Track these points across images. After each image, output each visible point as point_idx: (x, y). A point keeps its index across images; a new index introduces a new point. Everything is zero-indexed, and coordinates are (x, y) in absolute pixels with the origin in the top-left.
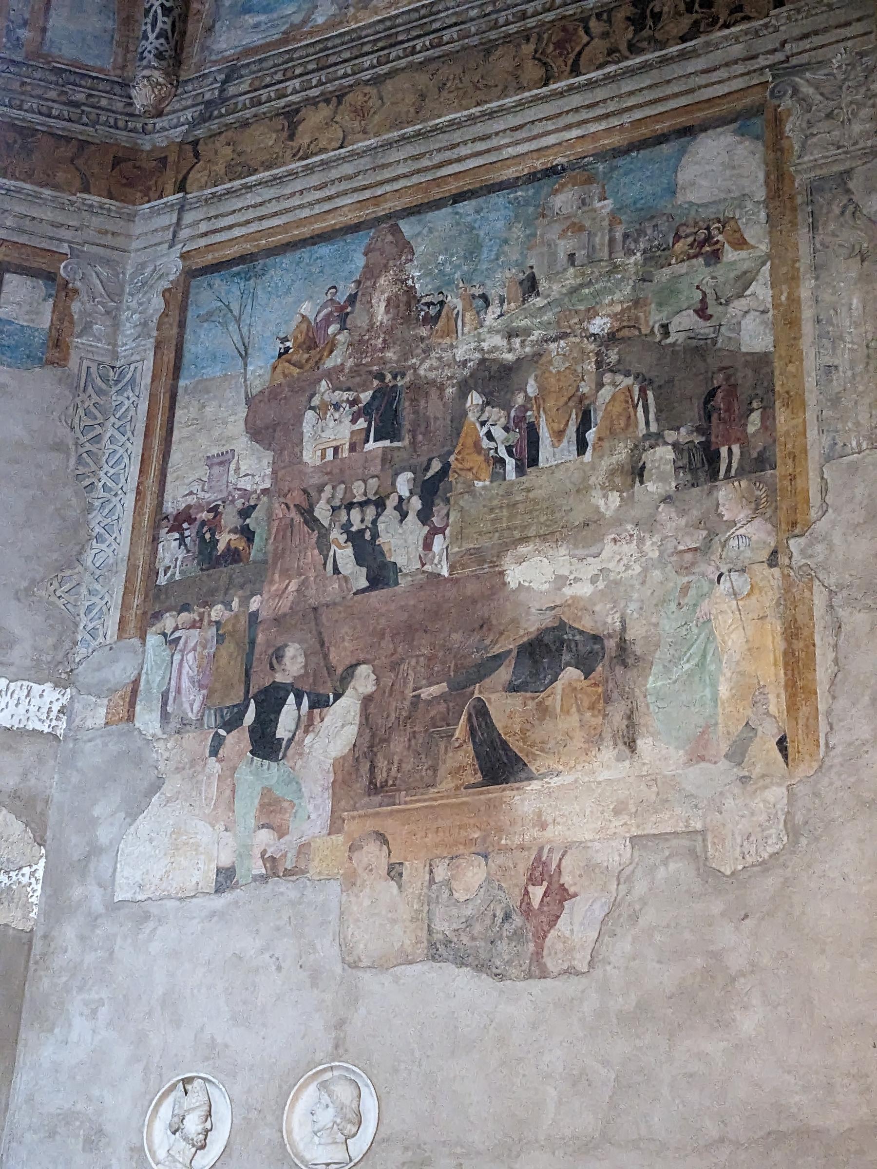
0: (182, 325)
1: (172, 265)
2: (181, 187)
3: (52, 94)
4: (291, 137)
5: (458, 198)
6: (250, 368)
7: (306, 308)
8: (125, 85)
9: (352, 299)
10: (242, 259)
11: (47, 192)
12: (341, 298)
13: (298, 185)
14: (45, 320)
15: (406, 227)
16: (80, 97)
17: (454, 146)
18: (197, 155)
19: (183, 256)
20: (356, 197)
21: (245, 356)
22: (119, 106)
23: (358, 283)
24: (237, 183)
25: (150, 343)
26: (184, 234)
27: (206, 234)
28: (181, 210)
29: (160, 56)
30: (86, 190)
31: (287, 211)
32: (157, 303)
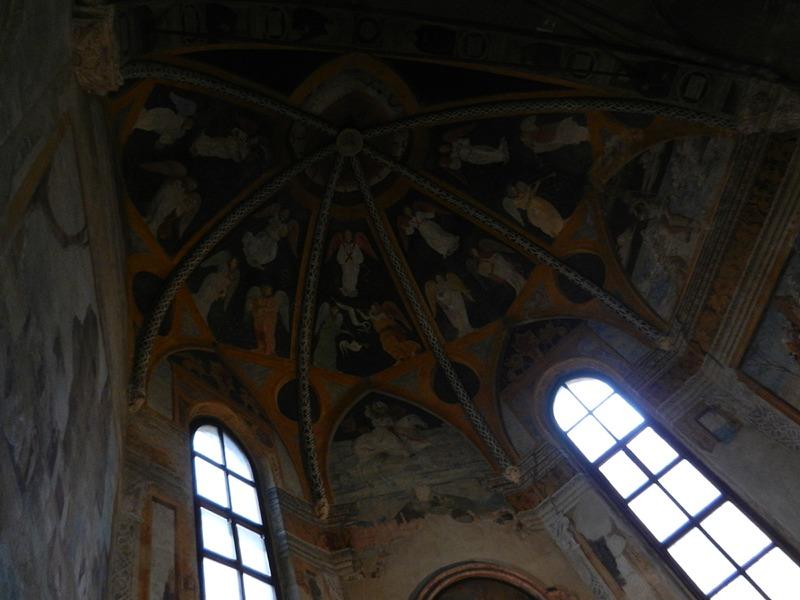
0: (756, 382)
1: (730, 372)
2: (704, 353)
4: (714, 311)
5: (783, 272)
6: (792, 370)
7: (784, 341)
8: (658, 349)
9: (793, 325)
10: (747, 350)
11: (679, 391)
12: (791, 328)
13: (734, 318)
14: (723, 420)
15: (780, 293)
16: (653, 363)
17: (761, 265)
18: (697, 343)
19: (730, 366)
20: (754, 303)
21: (786, 370)
22: (663, 355)
23: (789, 319)
24: (717, 336)
25: (755, 396)
26: (722, 362)
27: (728, 356)
28: (712, 357)
29: (657, 334)
30: (685, 380)
31: (741, 326)
32: (741, 384)
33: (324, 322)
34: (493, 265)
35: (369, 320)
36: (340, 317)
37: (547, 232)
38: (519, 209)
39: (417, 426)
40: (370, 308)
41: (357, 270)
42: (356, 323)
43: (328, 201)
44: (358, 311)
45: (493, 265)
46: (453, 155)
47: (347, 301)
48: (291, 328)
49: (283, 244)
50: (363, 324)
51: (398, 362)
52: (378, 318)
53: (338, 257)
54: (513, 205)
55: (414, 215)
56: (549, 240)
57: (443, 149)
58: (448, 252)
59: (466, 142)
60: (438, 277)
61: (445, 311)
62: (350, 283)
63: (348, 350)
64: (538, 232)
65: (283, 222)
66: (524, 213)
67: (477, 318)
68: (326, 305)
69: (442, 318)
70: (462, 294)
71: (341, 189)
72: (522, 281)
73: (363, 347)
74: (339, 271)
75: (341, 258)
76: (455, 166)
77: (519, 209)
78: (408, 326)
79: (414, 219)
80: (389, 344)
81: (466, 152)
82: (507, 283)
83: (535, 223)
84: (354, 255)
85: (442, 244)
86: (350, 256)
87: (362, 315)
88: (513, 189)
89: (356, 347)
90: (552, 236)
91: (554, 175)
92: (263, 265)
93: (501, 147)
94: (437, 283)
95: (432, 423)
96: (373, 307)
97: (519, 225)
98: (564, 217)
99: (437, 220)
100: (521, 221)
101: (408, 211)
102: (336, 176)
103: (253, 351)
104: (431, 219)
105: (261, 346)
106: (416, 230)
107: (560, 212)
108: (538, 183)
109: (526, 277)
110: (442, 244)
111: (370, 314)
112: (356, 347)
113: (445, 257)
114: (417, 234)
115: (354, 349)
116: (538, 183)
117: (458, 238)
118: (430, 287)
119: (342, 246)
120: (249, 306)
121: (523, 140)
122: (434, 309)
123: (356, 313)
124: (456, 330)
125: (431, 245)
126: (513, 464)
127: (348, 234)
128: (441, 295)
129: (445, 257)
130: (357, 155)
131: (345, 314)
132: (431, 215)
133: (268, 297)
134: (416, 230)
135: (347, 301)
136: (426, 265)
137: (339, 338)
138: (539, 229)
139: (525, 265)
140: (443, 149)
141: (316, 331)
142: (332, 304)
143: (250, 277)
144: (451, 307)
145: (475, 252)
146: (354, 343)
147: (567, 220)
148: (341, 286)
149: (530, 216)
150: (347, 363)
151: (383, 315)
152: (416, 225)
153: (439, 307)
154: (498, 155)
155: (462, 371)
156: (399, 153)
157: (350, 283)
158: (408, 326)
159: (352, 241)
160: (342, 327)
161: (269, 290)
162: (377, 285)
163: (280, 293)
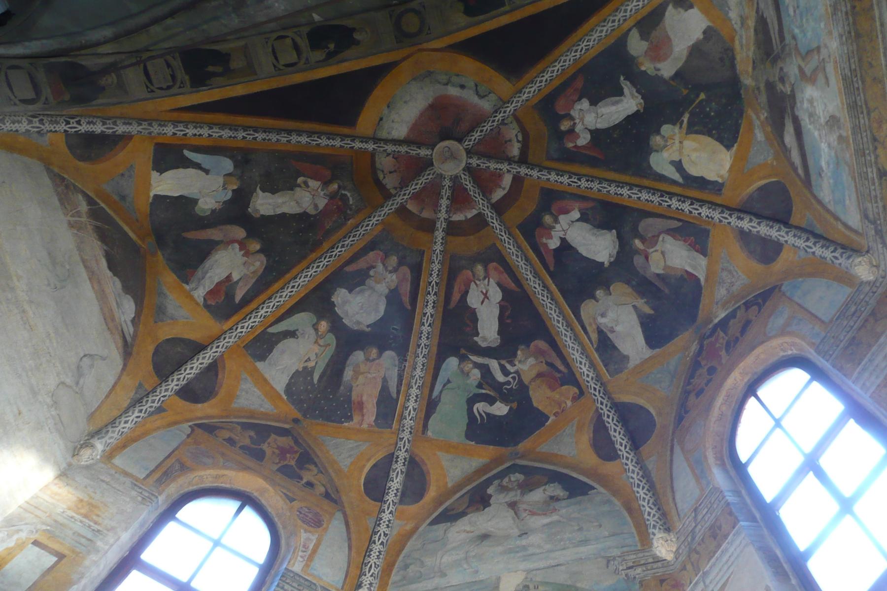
3: (845, 323)
33: (449, 381)
34: (663, 253)
35: (517, 372)
36: (476, 374)
37: (711, 176)
38: (673, 163)
39: (552, 498)
40: (515, 355)
41: (497, 312)
42: (501, 378)
43: (439, 234)
44: (503, 362)
45: (663, 253)
46: (579, 128)
47: (488, 352)
48: (398, 392)
49: (393, 297)
50: (509, 378)
51: (552, 418)
52: (526, 365)
53: (468, 300)
54: (661, 162)
55: (556, 221)
56: (716, 187)
57: (565, 126)
58: (610, 256)
59: (585, 104)
60: (599, 293)
61: (610, 335)
62: (488, 330)
63: (488, 414)
64: (701, 183)
65: (391, 272)
66: (678, 165)
67: (655, 333)
68: (452, 362)
69: (605, 345)
70: (634, 307)
71: (458, 217)
72: (703, 261)
73: (511, 409)
74: (473, 317)
75: (474, 300)
76: (584, 139)
77: (673, 163)
78: (562, 368)
79: (558, 227)
80: (540, 397)
81: (593, 117)
82: (687, 271)
83: (694, 171)
84: (490, 293)
85: (599, 246)
86: (486, 296)
87: (508, 366)
88: (658, 138)
89: (500, 409)
90: (720, 181)
91: (702, 96)
92: (368, 326)
93: (626, 91)
94: (597, 301)
95: (576, 489)
96: (519, 352)
97: (674, 182)
98: (728, 147)
99: (584, 218)
100: (677, 177)
101: (548, 219)
102: (444, 202)
103: (346, 424)
104: (578, 220)
105: (356, 418)
106: (563, 240)
107: (721, 142)
108: (686, 118)
109: (705, 254)
110: (599, 246)
111: (517, 363)
112: (500, 409)
113: (607, 264)
114: (565, 246)
115: (498, 413)
116: (686, 118)
117: (614, 231)
118: (588, 309)
119: (473, 285)
120: (348, 374)
121: (643, 68)
122: (594, 336)
123: (500, 364)
124: (626, 358)
125: (585, 254)
126: (668, 530)
127: (479, 268)
128: (603, 315)
129: (607, 264)
130: (464, 170)
131: (486, 371)
132: (576, 215)
133: (374, 360)
134: (563, 240)
135: (488, 352)
136: (580, 281)
137: (472, 401)
138: (702, 178)
139: (696, 236)
140: (565, 126)
141: (436, 393)
142: (463, 358)
143: (349, 341)
144: (618, 328)
145: (638, 243)
146: (498, 404)
147: (735, 148)
148: (477, 334)
149: (686, 166)
150: (481, 431)
151: (531, 361)
152: (561, 234)
153: (600, 332)
154: (629, 103)
155: (628, 414)
156: (515, 150)
157: (488, 330)
158: (562, 368)
159: (485, 278)
160: (480, 386)
161: (374, 352)
162: (522, 323)
163: (389, 354)
